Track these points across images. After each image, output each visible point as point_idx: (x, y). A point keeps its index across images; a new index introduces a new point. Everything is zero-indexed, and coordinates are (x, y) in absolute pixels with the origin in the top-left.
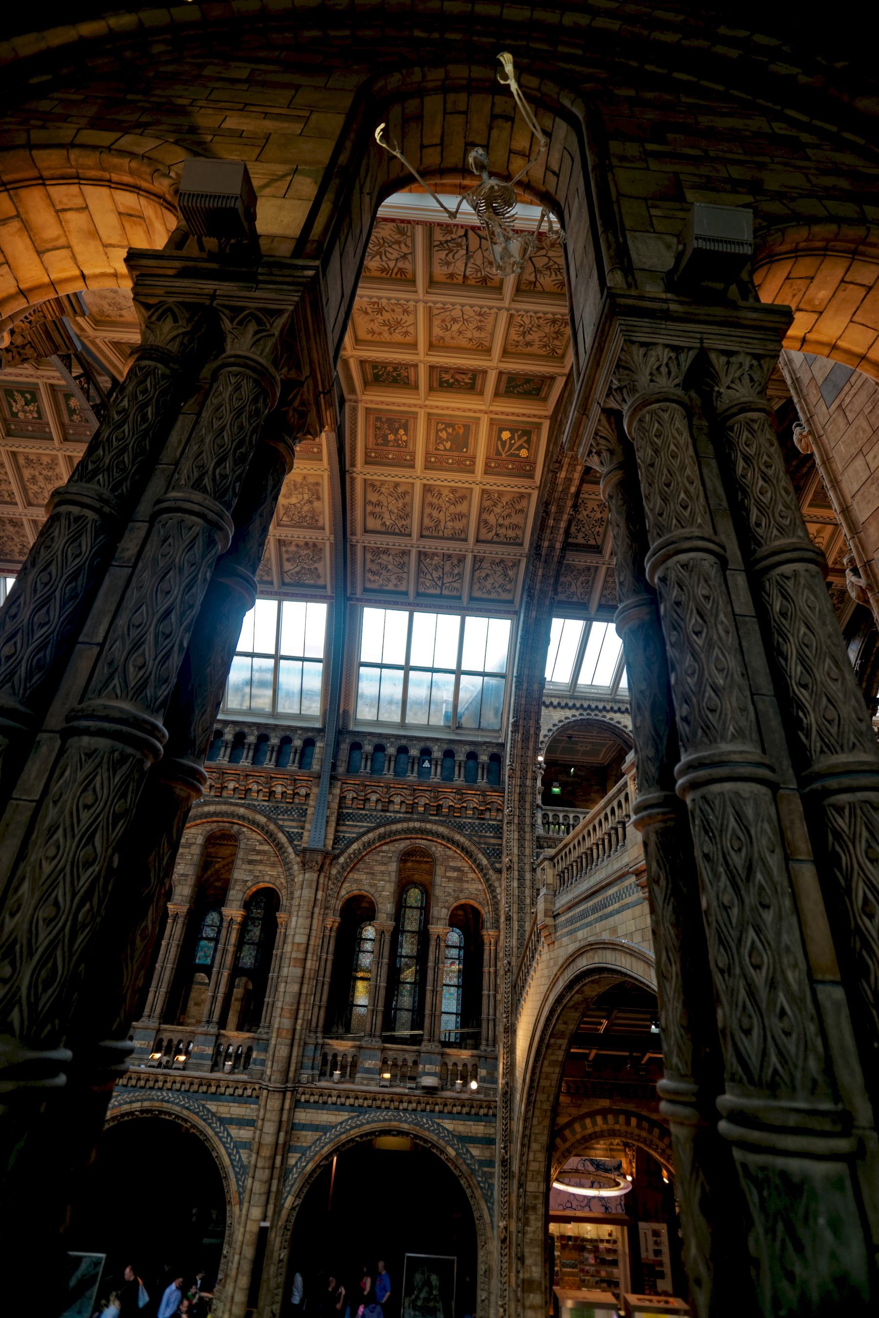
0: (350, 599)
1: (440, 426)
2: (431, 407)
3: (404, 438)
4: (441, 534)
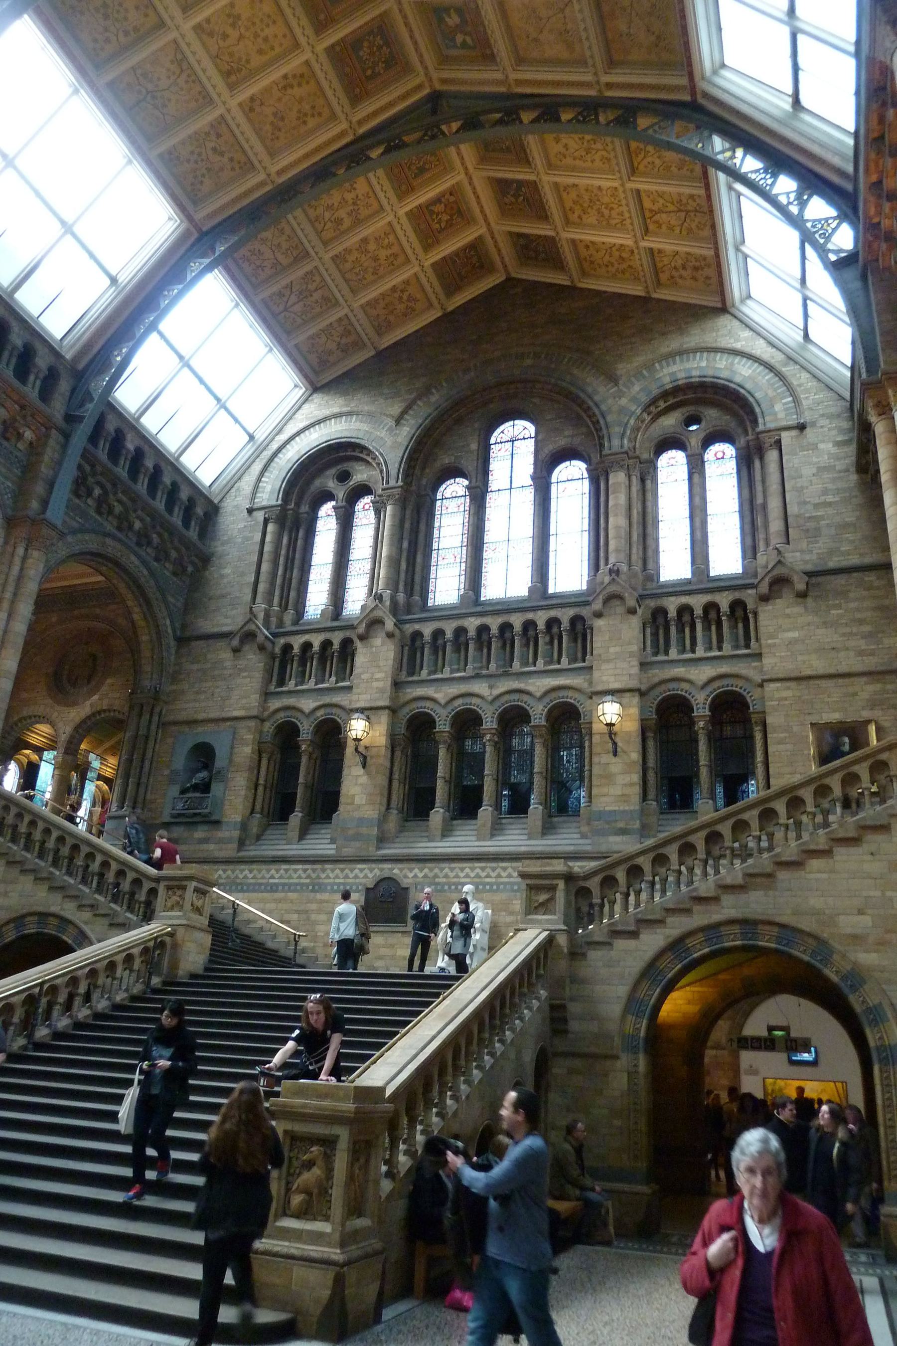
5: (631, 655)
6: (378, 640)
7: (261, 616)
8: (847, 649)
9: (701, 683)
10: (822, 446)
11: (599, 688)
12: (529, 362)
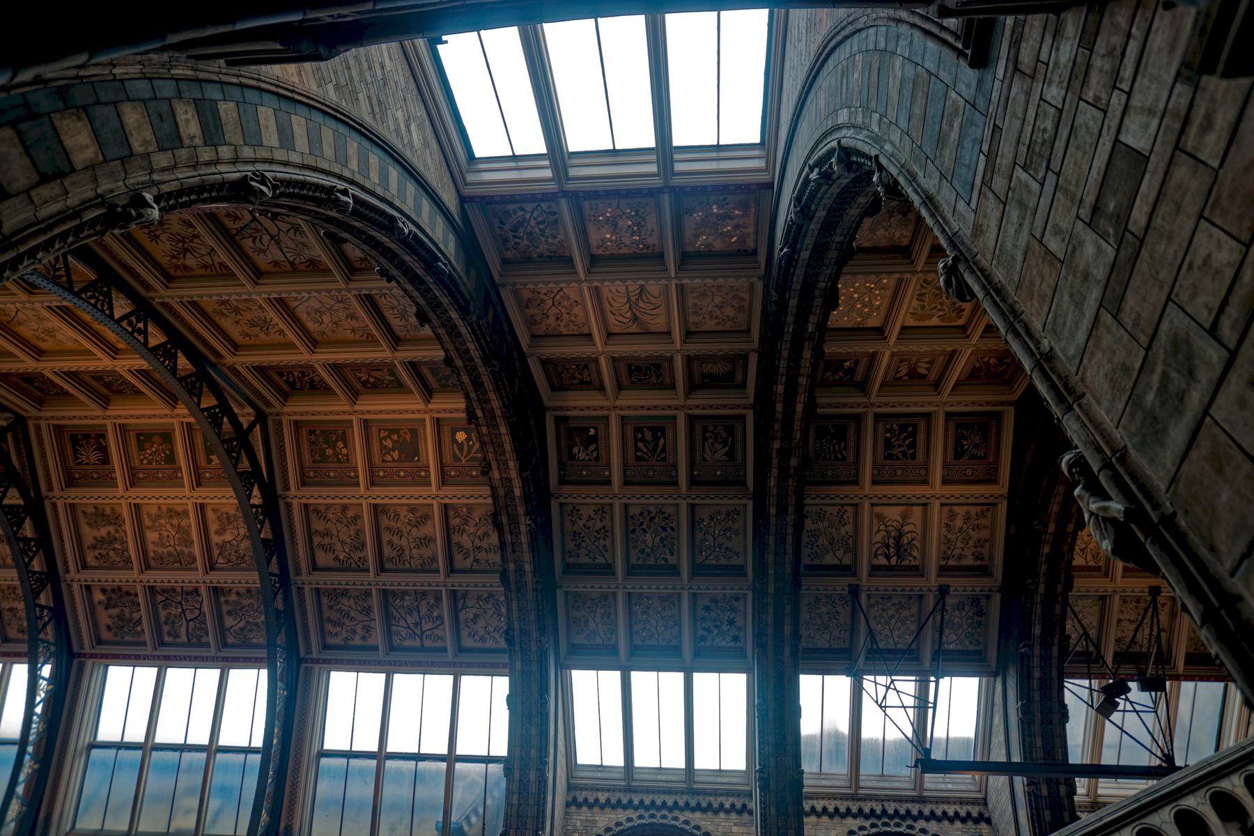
0: (306, 661)
1: (383, 434)
2: (362, 413)
3: (344, 451)
4: (407, 565)
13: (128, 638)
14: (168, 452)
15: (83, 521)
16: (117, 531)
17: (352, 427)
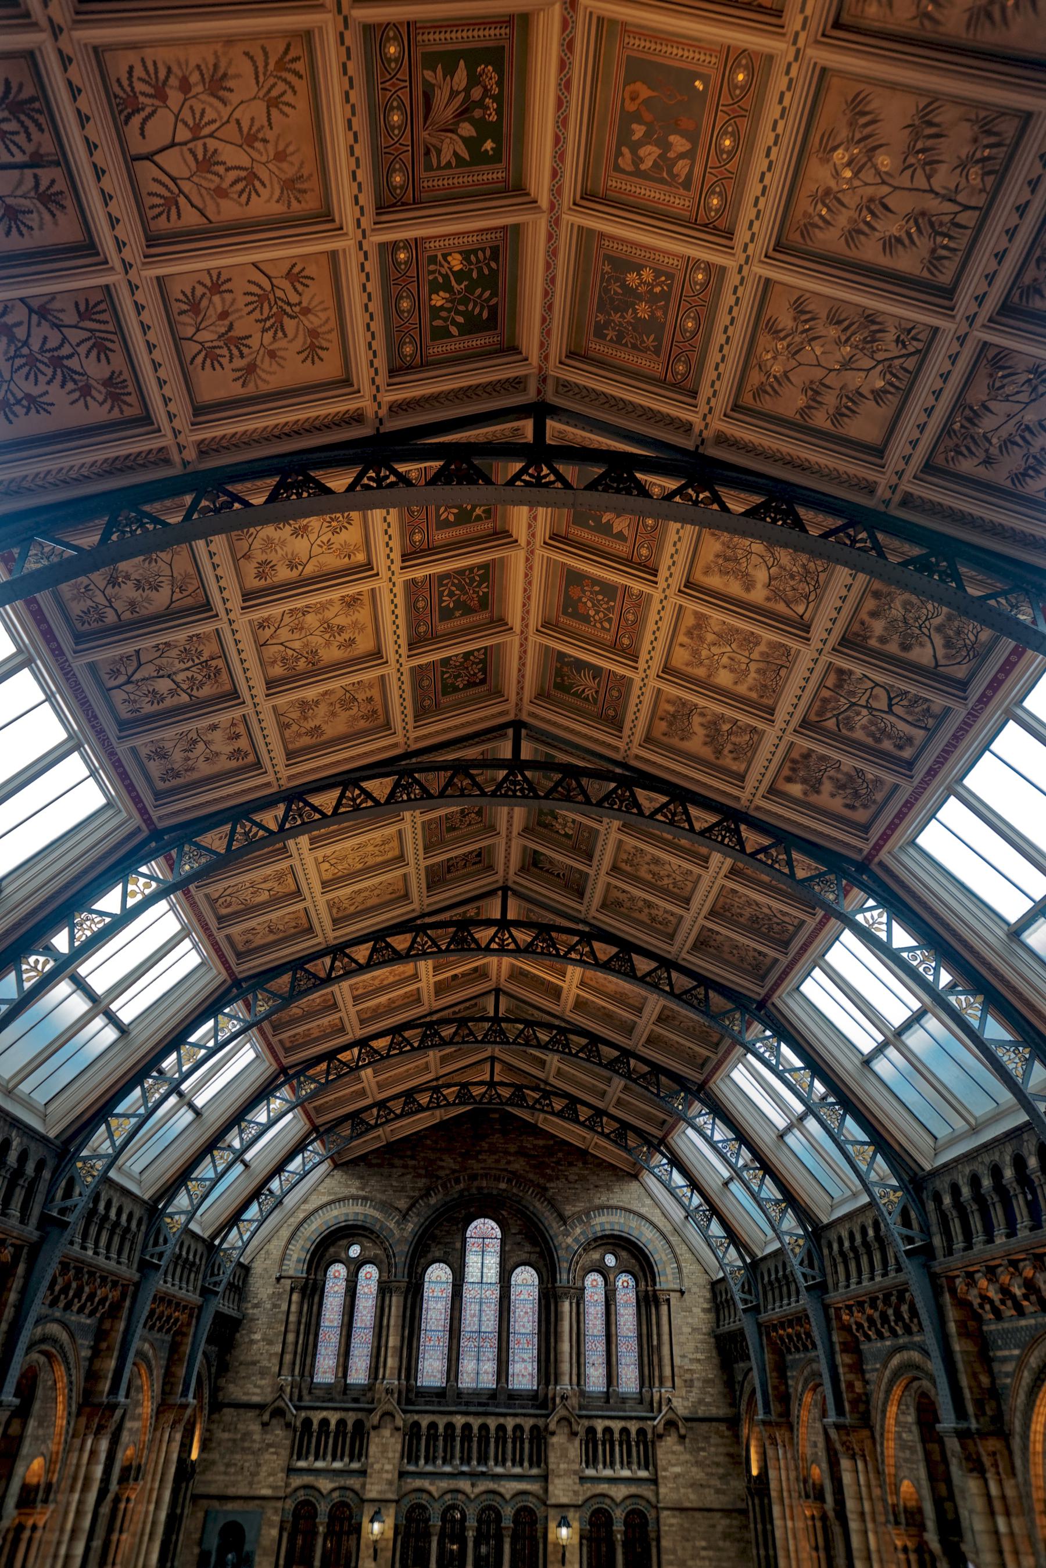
2: (556, 191)
3: (647, 275)
4: (968, 218)
5: (575, 1472)
6: (386, 1432)
7: (288, 1389)
8: (709, 1487)
9: (618, 1500)
10: (695, 1310)
11: (552, 1501)
12: (503, 1186)
13: (879, 797)
14: (597, 588)
15: (675, 741)
16: (702, 715)
17: (602, 235)
